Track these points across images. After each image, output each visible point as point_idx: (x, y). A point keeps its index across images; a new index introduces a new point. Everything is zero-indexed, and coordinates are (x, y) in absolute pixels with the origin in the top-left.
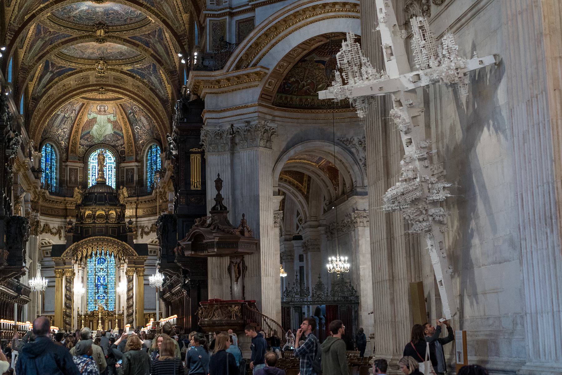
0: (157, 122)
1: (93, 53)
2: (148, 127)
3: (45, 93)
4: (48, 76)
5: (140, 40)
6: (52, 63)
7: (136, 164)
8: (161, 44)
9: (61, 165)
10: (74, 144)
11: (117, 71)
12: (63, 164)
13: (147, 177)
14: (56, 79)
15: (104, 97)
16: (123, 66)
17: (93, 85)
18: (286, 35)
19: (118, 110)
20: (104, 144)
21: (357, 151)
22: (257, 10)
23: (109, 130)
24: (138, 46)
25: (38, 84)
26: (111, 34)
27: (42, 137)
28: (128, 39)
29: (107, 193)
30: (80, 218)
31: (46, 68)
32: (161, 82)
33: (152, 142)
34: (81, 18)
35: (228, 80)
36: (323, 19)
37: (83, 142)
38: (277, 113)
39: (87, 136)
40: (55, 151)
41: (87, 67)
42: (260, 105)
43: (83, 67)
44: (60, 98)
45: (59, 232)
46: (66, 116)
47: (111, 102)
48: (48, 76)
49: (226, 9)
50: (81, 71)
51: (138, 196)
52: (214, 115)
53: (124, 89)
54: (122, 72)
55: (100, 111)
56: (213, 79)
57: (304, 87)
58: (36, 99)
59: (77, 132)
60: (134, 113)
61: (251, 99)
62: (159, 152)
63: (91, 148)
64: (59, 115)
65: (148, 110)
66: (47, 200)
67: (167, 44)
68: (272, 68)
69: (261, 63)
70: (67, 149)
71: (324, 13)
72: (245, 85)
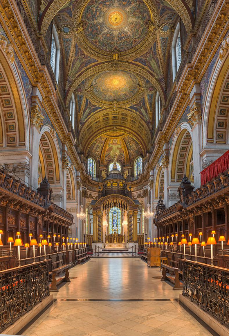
2: (136, 149)
4: (88, 110)
6: (89, 101)
7: (130, 167)
8: (154, 59)
9: (97, 169)
10: (103, 160)
11: (123, 108)
12: (98, 168)
13: (135, 173)
14: (92, 114)
15: (116, 135)
16: (126, 104)
19: (122, 144)
23: (118, 153)
27: (88, 154)
28: (133, 62)
33: (138, 156)
37: (107, 159)
40: (94, 162)
43: (106, 107)
46: (99, 145)
48: (88, 110)
50: (105, 109)
53: (125, 127)
54: (125, 109)
55: (114, 143)
59: (104, 153)
64: (96, 144)
66: (90, 183)
67: (159, 58)
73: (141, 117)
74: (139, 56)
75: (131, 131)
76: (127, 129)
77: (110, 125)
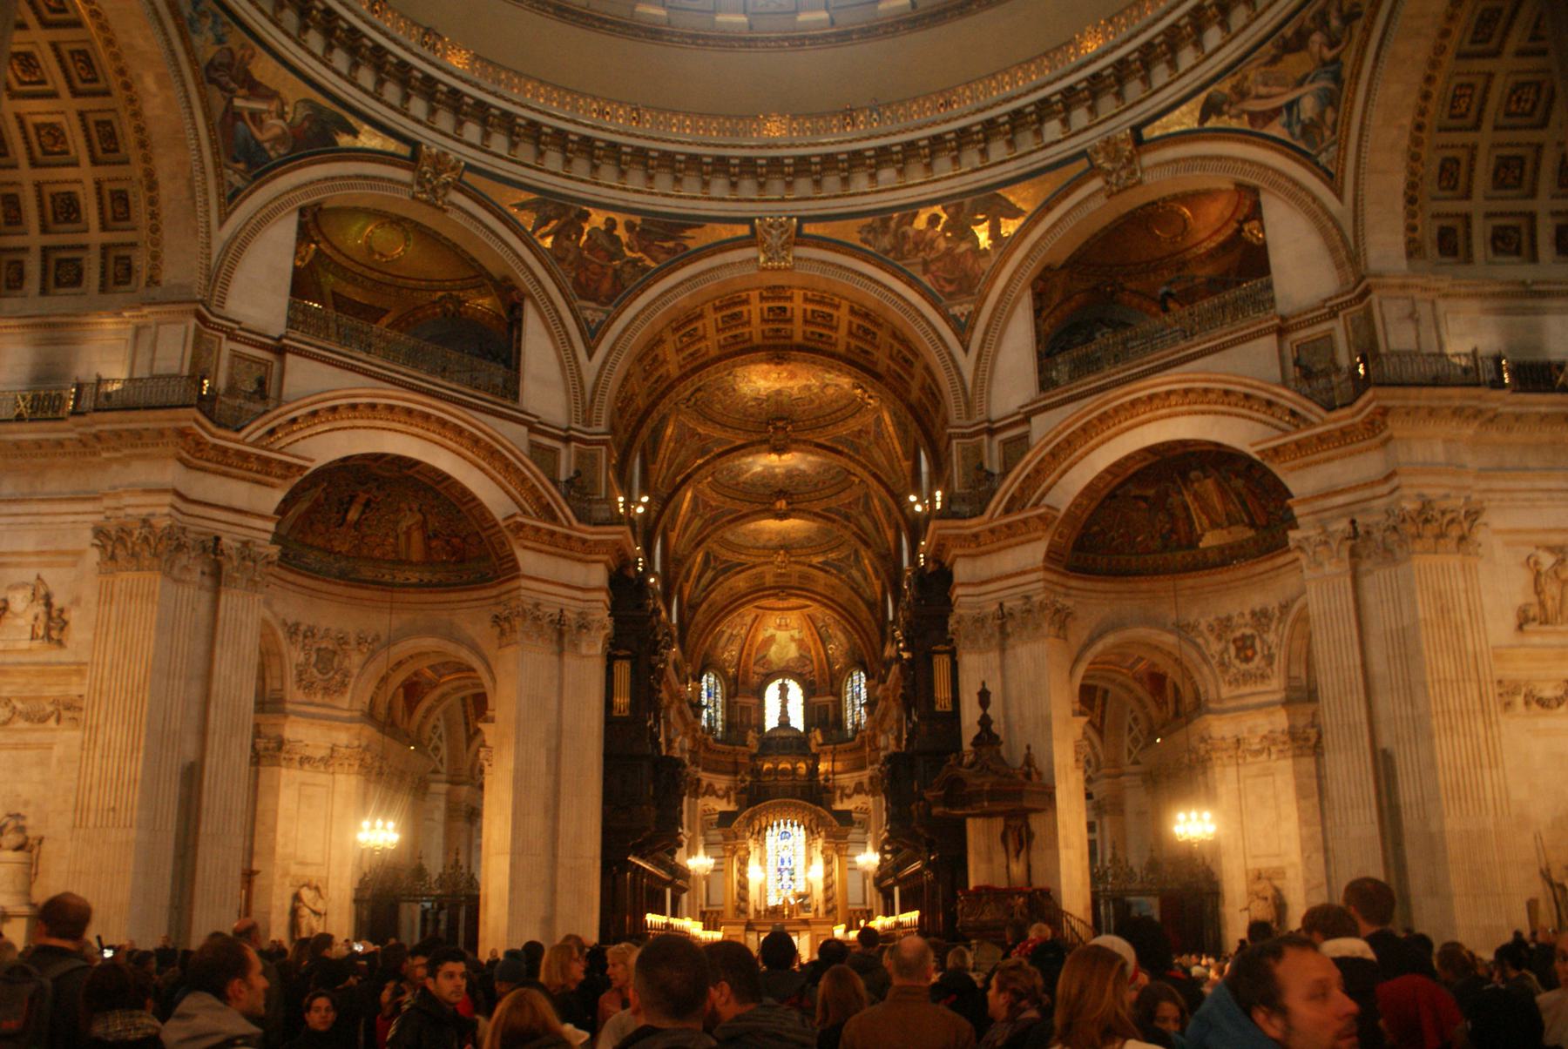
0: (861, 637)
1: (770, 540)
2: (847, 646)
3: (705, 598)
4: (709, 574)
5: (838, 513)
7: (831, 698)
10: (746, 673)
11: (804, 564)
14: (720, 579)
17: (771, 588)
18: (1087, 454)
20: (785, 672)
21: (1206, 641)
22: (1034, 420)
23: (793, 651)
24: (834, 521)
25: (696, 587)
26: (795, 506)
29: (794, 738)
30: (756, 773)
31: (706, 562)
32: (865, 576)
34: (754, 485)
35: (992, 531)
36: (1149, 421)
38: (1073, 583)
39: (763, 660)
41: (762, 559)
42: (1046, 569)
44: (726, 607)
45: (726, 795)
47: (796, 612)
48: (709, 574)
49: (982, 422)
50: (754, 566)
51: (835, 744)
52: (971, 590)
53: (813, 592)
54: (811, 566)
55: (780, 625)
56: (967, 532)
57: (1113, 539)
58: (694, 607)
59: (749, 655)
60: (827, 626)
62: (864, 680)
63: (769, 678)
65: (847, 620)
68: (1063, 509)
69: (1047, 500)
70: (736, 678)
71: (1151, 410)
72: (1022, 538)
73: (852, 588)
74: (834, 505)
75: (830, 603)
76: (819, 598)
77: (767, 585)
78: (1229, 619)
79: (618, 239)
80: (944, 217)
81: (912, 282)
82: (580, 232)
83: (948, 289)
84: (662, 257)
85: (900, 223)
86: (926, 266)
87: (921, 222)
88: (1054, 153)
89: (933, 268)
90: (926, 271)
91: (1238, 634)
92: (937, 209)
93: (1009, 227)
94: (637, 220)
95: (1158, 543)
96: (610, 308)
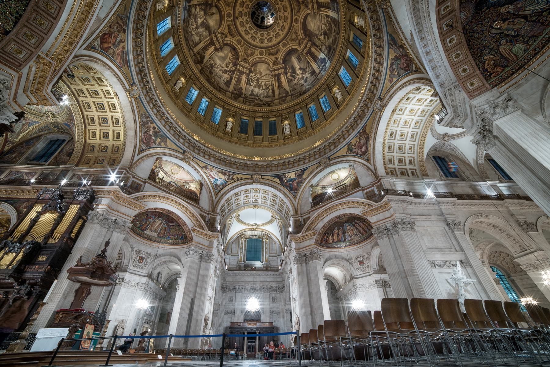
61: (130, 214)
78: (141, 251)
79: (120, 44)
80: (156, 130)
81: (141, 132)
82: (119, 31)
83: (144, 141)
84: (118, 61)
85: (149, 121)
86: (145, 132)
87: (152, 125)
88: (180, 145)
89: (146, 134)
90: (144, 133)
91: (141, 255)
92: (157, 127)
93: (163, 144)
94: (126, 49)
95: (138, 226)
96: (100, 50)
